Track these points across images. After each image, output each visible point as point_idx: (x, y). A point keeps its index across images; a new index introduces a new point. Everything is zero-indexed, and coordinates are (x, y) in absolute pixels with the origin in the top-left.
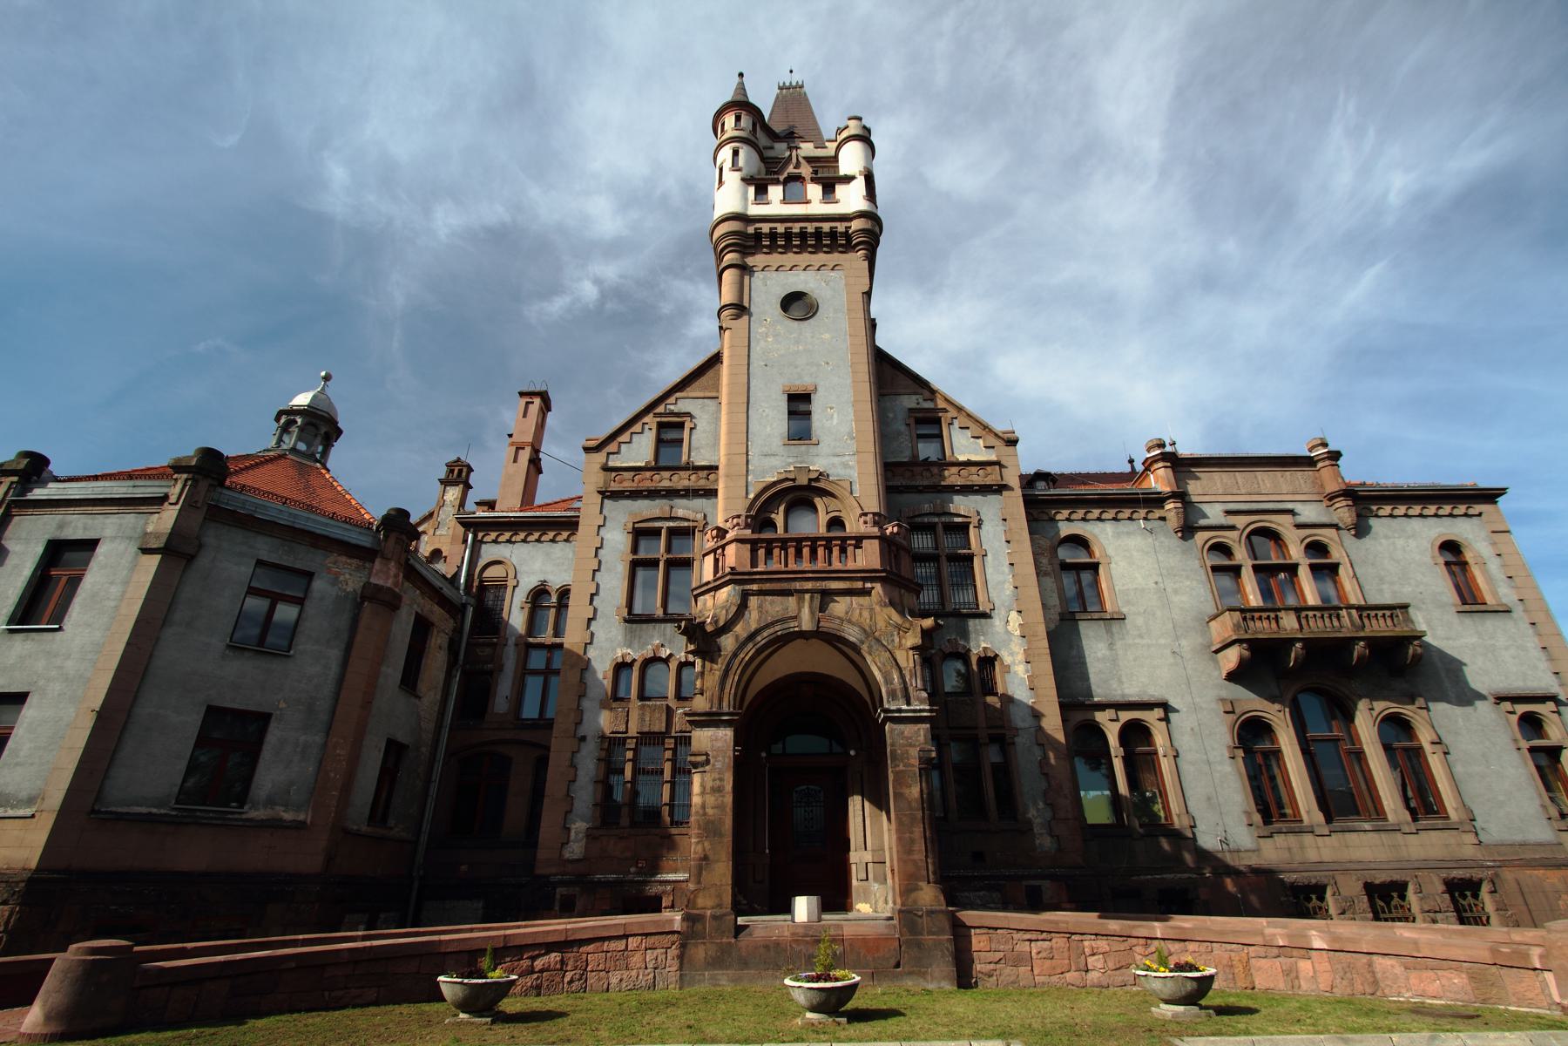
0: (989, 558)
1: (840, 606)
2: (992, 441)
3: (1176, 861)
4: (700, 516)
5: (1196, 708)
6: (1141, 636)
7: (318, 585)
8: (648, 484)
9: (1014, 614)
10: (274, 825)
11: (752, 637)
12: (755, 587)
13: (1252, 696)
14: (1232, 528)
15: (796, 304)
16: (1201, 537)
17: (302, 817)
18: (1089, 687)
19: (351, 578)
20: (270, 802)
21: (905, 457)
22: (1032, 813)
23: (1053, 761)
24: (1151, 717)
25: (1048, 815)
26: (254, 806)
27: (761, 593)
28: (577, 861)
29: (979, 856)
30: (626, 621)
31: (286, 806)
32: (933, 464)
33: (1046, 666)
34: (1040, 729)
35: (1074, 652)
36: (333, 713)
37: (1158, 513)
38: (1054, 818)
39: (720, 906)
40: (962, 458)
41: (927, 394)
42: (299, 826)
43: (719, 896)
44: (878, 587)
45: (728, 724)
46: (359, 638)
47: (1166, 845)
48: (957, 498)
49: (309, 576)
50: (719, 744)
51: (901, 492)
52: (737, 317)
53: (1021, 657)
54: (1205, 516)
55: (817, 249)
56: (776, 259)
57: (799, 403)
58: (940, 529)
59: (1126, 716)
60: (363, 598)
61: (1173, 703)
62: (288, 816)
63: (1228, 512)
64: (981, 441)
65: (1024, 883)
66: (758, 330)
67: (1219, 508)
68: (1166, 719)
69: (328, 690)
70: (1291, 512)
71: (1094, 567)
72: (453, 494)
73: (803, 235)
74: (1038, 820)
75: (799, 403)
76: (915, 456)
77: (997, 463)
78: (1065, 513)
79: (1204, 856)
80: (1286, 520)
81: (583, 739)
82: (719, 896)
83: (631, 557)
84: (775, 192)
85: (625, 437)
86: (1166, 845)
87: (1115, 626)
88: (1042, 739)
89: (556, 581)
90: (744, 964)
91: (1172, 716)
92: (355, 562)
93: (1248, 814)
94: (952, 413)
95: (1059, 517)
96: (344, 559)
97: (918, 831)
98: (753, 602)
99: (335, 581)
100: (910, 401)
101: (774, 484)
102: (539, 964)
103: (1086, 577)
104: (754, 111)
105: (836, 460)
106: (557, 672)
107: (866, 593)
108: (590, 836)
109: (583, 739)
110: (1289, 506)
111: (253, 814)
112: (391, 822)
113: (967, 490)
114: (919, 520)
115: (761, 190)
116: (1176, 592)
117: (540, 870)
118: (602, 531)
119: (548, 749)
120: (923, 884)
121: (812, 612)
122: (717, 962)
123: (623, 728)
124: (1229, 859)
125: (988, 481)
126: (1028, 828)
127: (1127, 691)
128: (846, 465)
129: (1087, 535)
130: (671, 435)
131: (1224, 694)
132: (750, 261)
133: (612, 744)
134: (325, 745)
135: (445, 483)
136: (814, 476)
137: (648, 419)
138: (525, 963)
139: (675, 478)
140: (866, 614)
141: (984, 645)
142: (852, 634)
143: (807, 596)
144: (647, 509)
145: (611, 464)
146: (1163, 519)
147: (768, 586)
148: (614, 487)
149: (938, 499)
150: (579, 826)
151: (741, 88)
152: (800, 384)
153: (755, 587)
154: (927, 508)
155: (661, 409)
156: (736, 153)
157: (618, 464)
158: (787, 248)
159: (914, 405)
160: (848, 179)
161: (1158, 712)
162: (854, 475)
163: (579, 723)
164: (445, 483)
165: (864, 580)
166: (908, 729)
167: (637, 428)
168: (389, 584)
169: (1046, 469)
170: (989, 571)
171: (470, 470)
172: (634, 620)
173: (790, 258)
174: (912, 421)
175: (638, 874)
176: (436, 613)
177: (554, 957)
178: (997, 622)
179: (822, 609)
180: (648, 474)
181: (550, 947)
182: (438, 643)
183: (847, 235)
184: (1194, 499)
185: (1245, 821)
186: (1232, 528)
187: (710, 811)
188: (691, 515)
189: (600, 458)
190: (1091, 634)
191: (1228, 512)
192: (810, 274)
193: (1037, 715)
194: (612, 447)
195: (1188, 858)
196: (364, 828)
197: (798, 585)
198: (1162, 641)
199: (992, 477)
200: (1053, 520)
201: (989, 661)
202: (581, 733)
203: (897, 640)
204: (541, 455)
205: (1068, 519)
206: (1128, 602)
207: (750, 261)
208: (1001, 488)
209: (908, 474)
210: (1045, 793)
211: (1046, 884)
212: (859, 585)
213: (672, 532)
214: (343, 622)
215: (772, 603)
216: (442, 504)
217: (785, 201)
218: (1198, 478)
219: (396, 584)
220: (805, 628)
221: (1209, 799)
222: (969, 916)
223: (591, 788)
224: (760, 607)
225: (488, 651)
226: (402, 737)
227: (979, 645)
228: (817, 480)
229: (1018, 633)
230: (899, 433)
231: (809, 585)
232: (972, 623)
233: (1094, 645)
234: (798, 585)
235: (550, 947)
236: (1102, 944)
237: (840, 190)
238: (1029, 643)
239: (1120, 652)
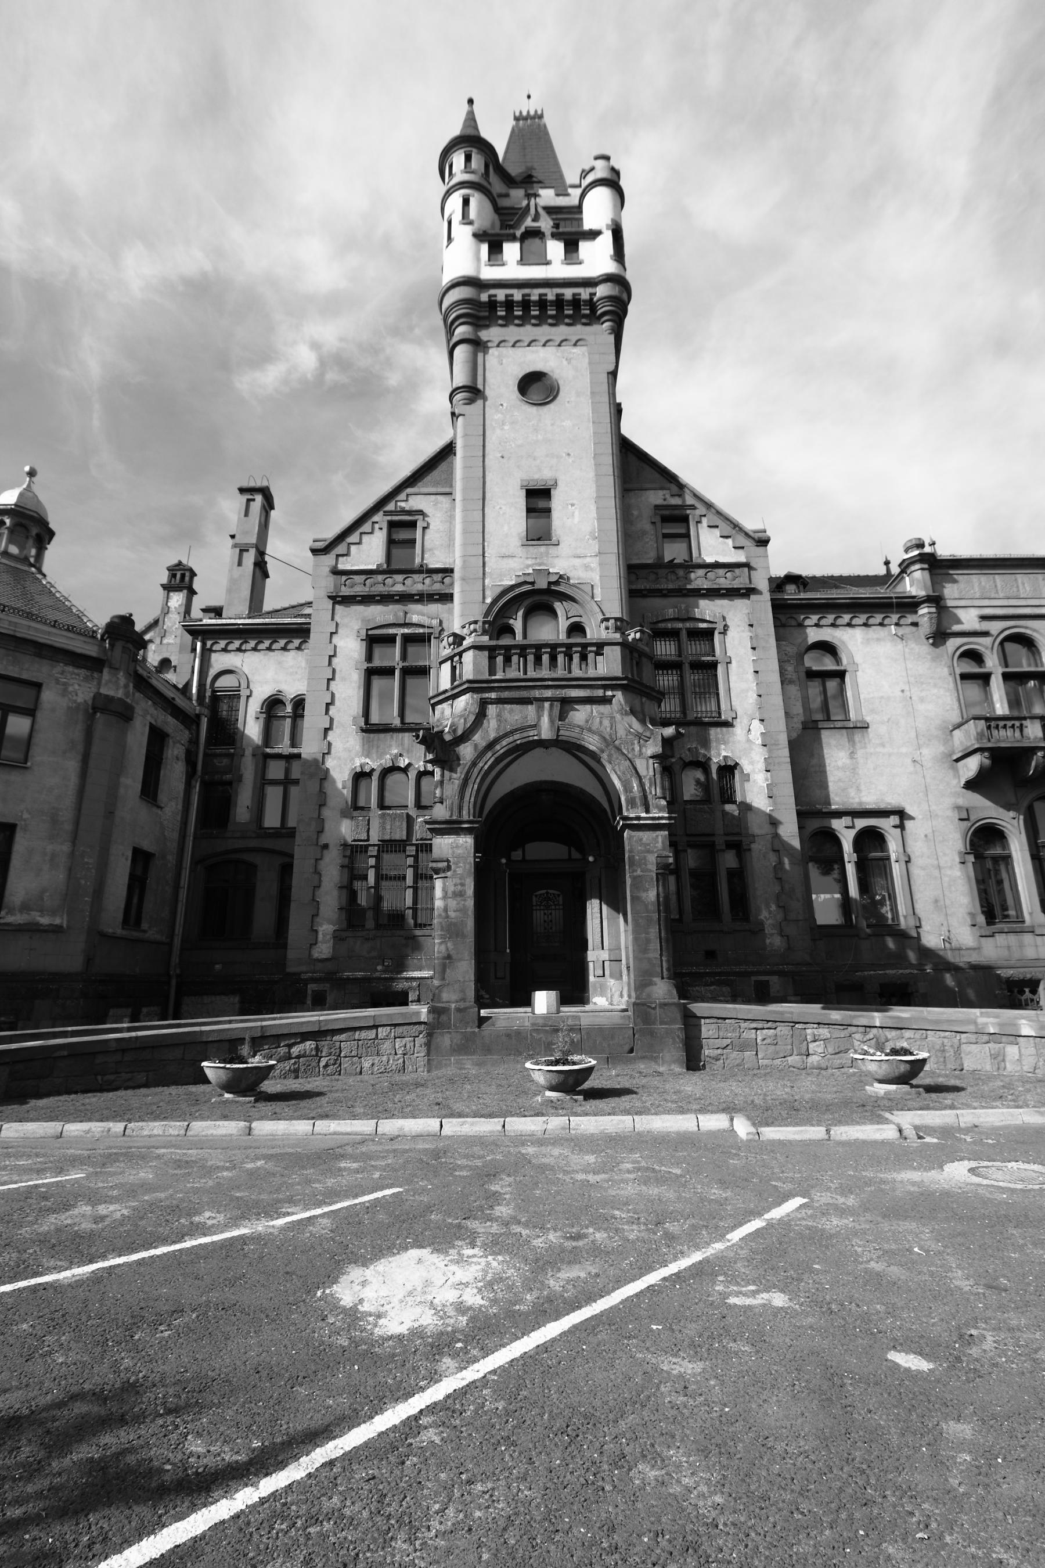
0: (733, 667)
1: (580, 715)
2: (742, 540)
3: (899, 958)
4: (435, 622)
5: (931, 815)
6: (883, 745)
7: (47, 696)
8: (380, 589)
9: (756, 723)
10: (32, 929)
11: (490, 746)
12: (493, 695)
13: (987, 803)
14: (986, 634)
15: (535, 386)
16: (953, 643)
17: (57, 921)
18: (828, 796)
19: (81, 689)
20: (25, 907)
21: (649, 559)
22: (764, 915)
23: (787, 866)
24: (887, 825)
25: (780, 916)
26: (11, 912)
27: (499, 701)
28: (326, 960)
29: (710, 954)
30: (363, 730)
31: (42, 911)
32: (680, 566)
33: (785, 774)
34: (776, 836)
35: (814, 761)
36: (77, 823)
37: (910, 618)
38: (785, 919)
39: (464, 1000)
40: (709, 559)
41: (675, 489)
42: (57, 930)
43: (463, 991)
44: (619, 695)
45: (468, 831)
46: (95, 749)
47: (891, 943)
48: (703, 603)
49: (38, 686)
50: (460, 851)
51: (644, 596)
52: (470, 401)
53: (761, 765)
54: (959, 622)
55: (558, 320)
56: (512, 332)
57: (538, 499)
58: (684, 634)
59: (861, 823)
60: (95, 709)
61: (909, 810)
62: (45, 921)
63: (984, 618)
64: (730, 541)
65: (753, 978)
66: (493, 416)
67: (974, 613)
68: (901, 827)
69: (69, 801)
71: (841, 675)
72: (177, 600)
73: (542, 303)
74: (770, 921)
75: (538, 499)
76: (660, 557)
77: (747, 565)
78: (814, 618)
79: (926, 953)
81: (326, 846)
82: (463, 991)
83: (365, 665)
84: (511, 250)
85: (354, 538)
86: (891, 943)
87: (858, 736)
88: (778, 846)
89: (291, 689)
90: (488, 1050)
91: (908, 824)
92: (83, 672)
93: (972, 915)
94: (702, 509)
95: (807, 622)
96: (70, 669)
97: (654, 931)
98: (492, 710)
99: (64, 693)
100: (656, 497)
101: (512, 588)
102: (295, 1050)
103: (832, 685)
104: (487, 149)
105: (577, 562)
106: (296, 782)
107: (606, 701)
109: (326, 846)
111: (10, 919)
112: (145, 926)
113: (714, 593)
114: (662, 625)
115: (496, 249)
116: (922, 700)
117: (291, 969)
118: (336, 639)
119: (292, 856)
120: (657, 980)
121: (552, 721)
122: (464, 1048)
123: (364, 836)
124: (950, 957)
125: (736, 584)
126: (759, 930)
127: (864, 799)
128: (587, 567)
129: (835, 642)
130: (402, 535)
131: (961, 802)
132: (484, 335)
133: (354, 851)
134: (73, 853)
135: (168, 588)
136: (553, 579)
137: (378, 517)
138: (282, 1051)
139: (408, 582)
140: (606, 723)
141: (724, 753)
142: (592, 743)
143: (547, 705)
144: (380, 614)
145: (341, 567)
146: (915, 624)
147: (506, 694)
148: (345, 591)
149: (682, 603)
150: (326, 929)
151: (471, 119)
152: (540, 476)
153: (493, 695)
154: (671, 613)
155: (391, 507)
156: (466, 202)
157: (348, 567)
158: (524, 320)
159: (660, 502)
160: (593, 235)
161: (894, 820)
162: (595, 577)
163: (321, 831)
164: (168, 588)
165: (605, 687)
166: (646, 836)
167: (366, 527)
168: (120, 694)
169: (797, 571)
170: (732, 678)
171: (193, 574)
172: (370, 729)
173: (528, 332)
174: (658, 519)
175: (384, 971)
176: (170, 724)
177: (309, 1045)
178: (739, 730)
179: (562, 717)
180: (380, 578)
181: (305, 1036)
182: (175, 753)
183: (591, 304)
184: (950, 603)
185: (969, 921)
186: (986, 634)
187: (452, 914)
188: (426, 621)
189: (329, 560)
190: (833, 742)
191: (984, 618)
192: (550, 351)
193: (774, 823)
194: (341, 549)
195: (912, 956)
196: (119, 932)
197: (537, 693)
198: (904, 750)
199: (739, 580)
200: (801, 625)
201: (729, 770)
202: (323, 840)
203: (637, 748)
204: (267, 558)
205: (817, 625)
206: (873, 711)
207: (484, 335)
208: (748, 592)
209: (652, 577)
210: (778, 897)
211: (774, 980)
212: (600, 693)
213: (408, 639)
214: (77, 733)
215: (511, 711)
216: (166, 610)
217: (522, 261)
218: (955, 581)
219: (127, 694)
220: (544, 736)
221: (936, 901)
222: (699, 1008)
223: (336, 893)
224: (499, 715)
225: (225, 761)
226: (146, 845)
227: (719, 753)
228: (557, 583)
229: (759, 742)
230: (644, 533)
231: (548, 693)
232: (713, 732)
233: (835, 754)
234: (537, 693)
235: (305, 1036)
236: (824, 1032)
237: (584, 246)
238: (770, 751)
239: (861, 761)
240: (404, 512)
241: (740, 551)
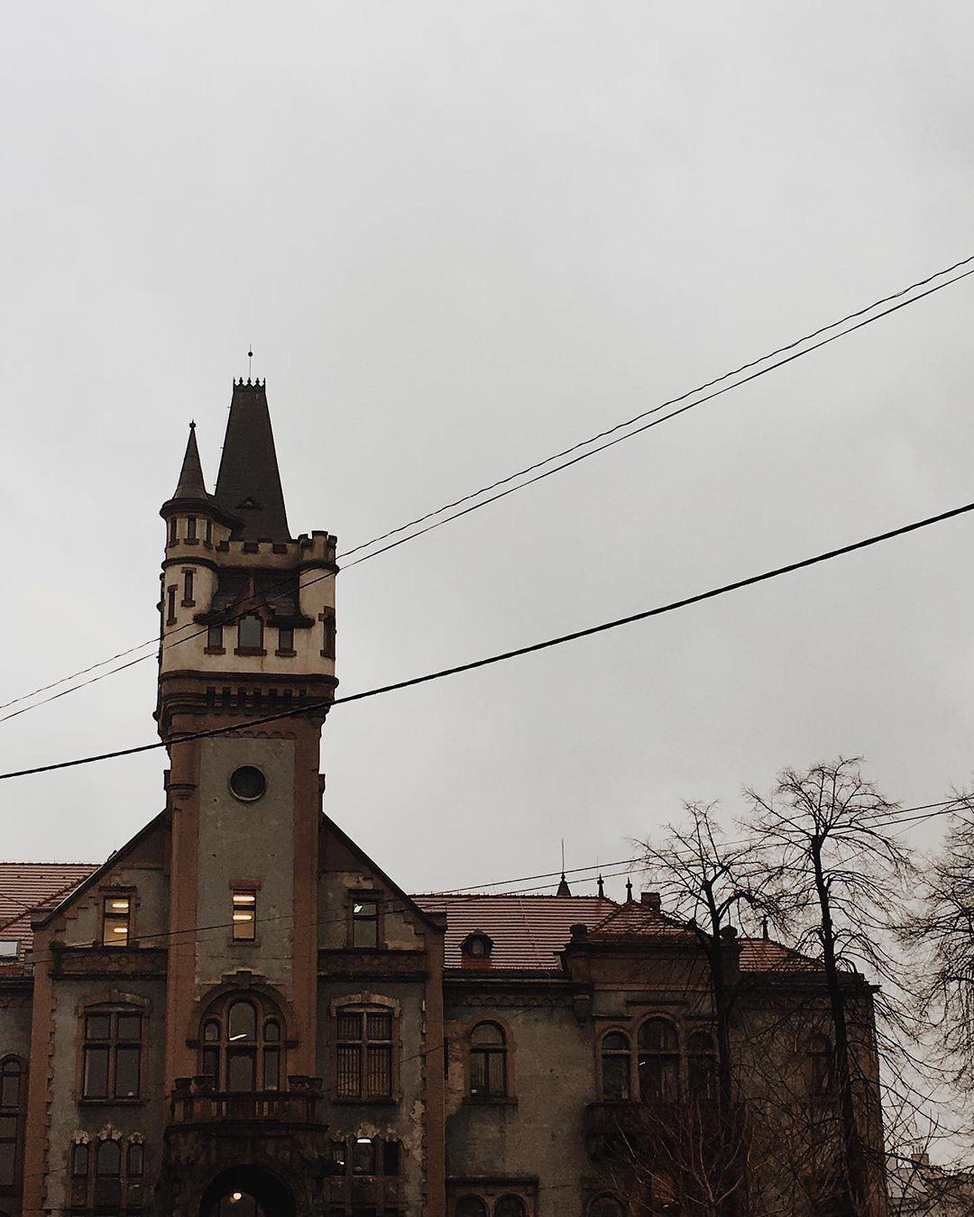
40: (391, 945)
59: (501, 1192)
68: (535, 1195)
84: (230, 638)
94: (388, 896)
100: (349, 881)
118: (55, 1016)
141: (390, 1131)
154: (357, 998)
161: (530, 1189)
163: (44, 1199)
189: (48, 937)
217: (239, 652)
241: (422, 938)
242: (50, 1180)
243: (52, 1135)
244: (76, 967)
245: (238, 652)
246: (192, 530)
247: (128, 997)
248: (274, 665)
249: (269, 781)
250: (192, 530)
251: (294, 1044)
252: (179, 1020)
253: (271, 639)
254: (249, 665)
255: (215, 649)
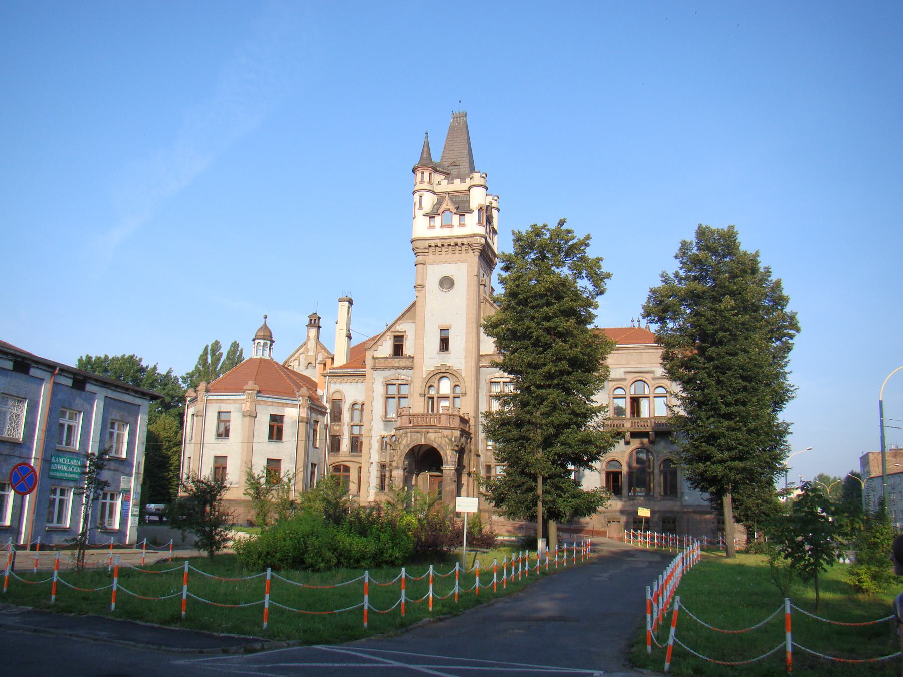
1: (432, 436)
8: (390, 365)
14: (624, 380)
27: (411, 432)
67: (623, 370)
70: (653, 372)
72: (313, 332)
80: (650, 376)
84: (438, 220)
89: (360, 400)
108: (376, 495)
110: (653, 369)
135: (310, 326)
137: (388, 334)
154: (497, 375)
164: (310, 326)
171: (319, 318)
186: (624, 380)
216: (308, 338)
217: (442, 226)
240: (398, 331)
242: (372, 451)
243: (373, 433)
244: (382, 364)
245: (442, 226)
246: (422, 177)
247: (403, 377)
248: (456, 231)
249: (455, 282)
250: (422, 177)
251: (464, 394)
252: (418, 387)
253: (455, 219)
254: (446, 232)
255: (431, 227)
